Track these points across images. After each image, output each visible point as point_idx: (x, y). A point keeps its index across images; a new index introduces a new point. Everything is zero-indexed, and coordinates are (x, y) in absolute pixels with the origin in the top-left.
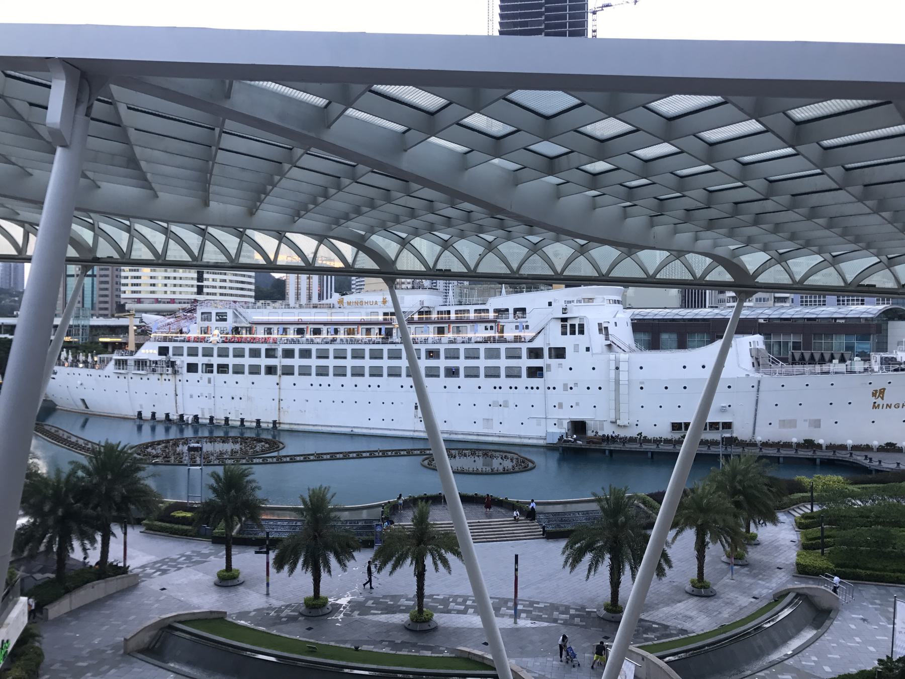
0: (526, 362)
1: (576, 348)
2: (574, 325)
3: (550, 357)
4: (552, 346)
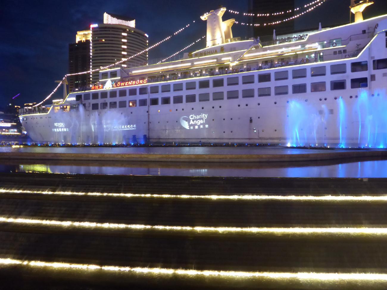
4: (377, 58)
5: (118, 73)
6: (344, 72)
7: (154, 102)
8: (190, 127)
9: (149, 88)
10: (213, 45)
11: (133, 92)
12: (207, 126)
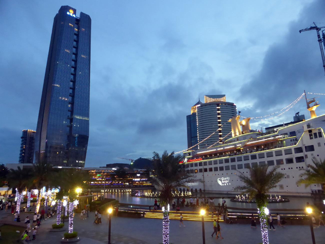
0: (295, 155)
1: (319, 144)
2: (316, 133)
3: (306, 151)
4: (306, 146)
5: (191, 154)
6: (292, 153)
7: (206, 170)
8: (222, 184)
9: (203, 163)
10: (235, 136)
11: (196, 165)
12: (230, 184)
